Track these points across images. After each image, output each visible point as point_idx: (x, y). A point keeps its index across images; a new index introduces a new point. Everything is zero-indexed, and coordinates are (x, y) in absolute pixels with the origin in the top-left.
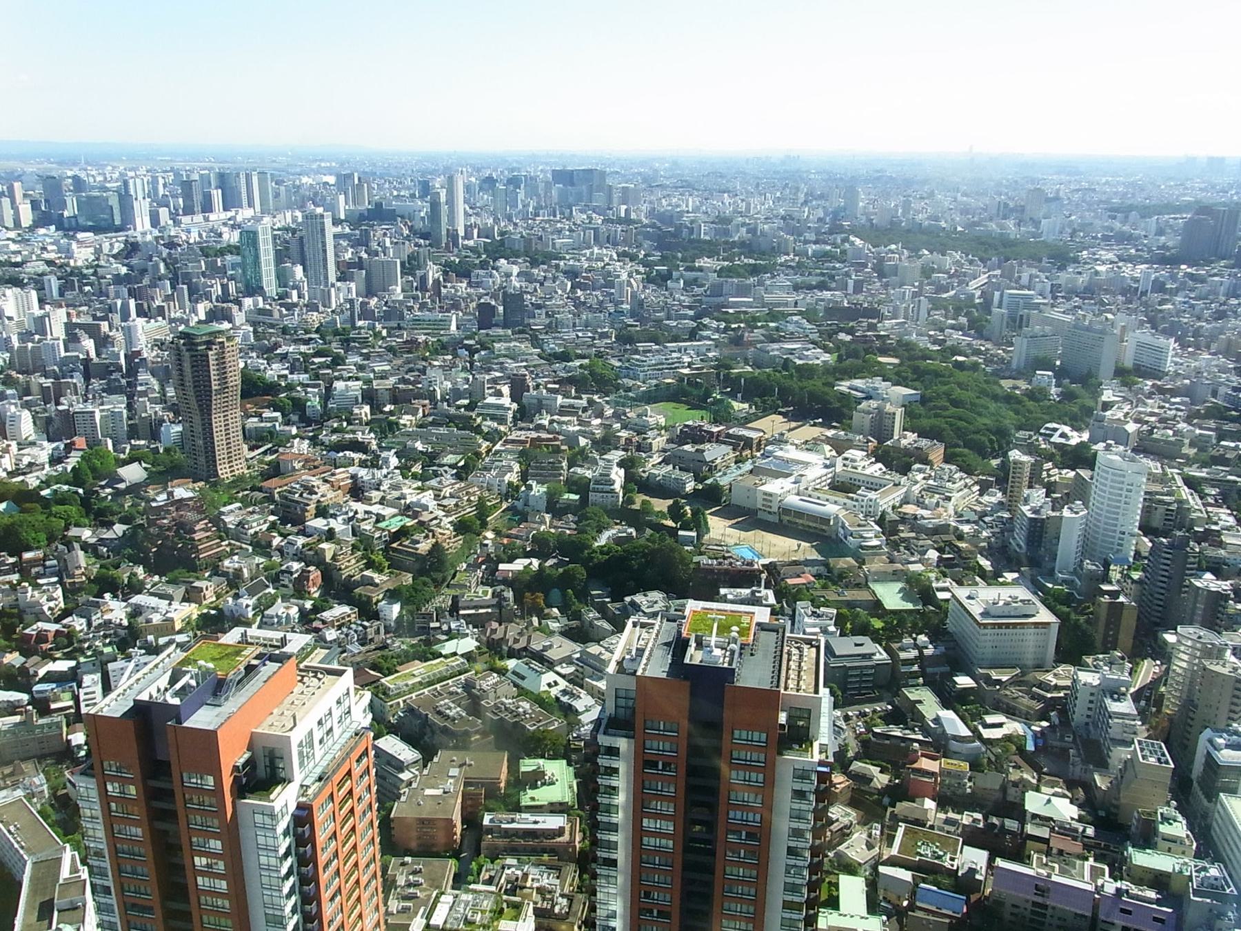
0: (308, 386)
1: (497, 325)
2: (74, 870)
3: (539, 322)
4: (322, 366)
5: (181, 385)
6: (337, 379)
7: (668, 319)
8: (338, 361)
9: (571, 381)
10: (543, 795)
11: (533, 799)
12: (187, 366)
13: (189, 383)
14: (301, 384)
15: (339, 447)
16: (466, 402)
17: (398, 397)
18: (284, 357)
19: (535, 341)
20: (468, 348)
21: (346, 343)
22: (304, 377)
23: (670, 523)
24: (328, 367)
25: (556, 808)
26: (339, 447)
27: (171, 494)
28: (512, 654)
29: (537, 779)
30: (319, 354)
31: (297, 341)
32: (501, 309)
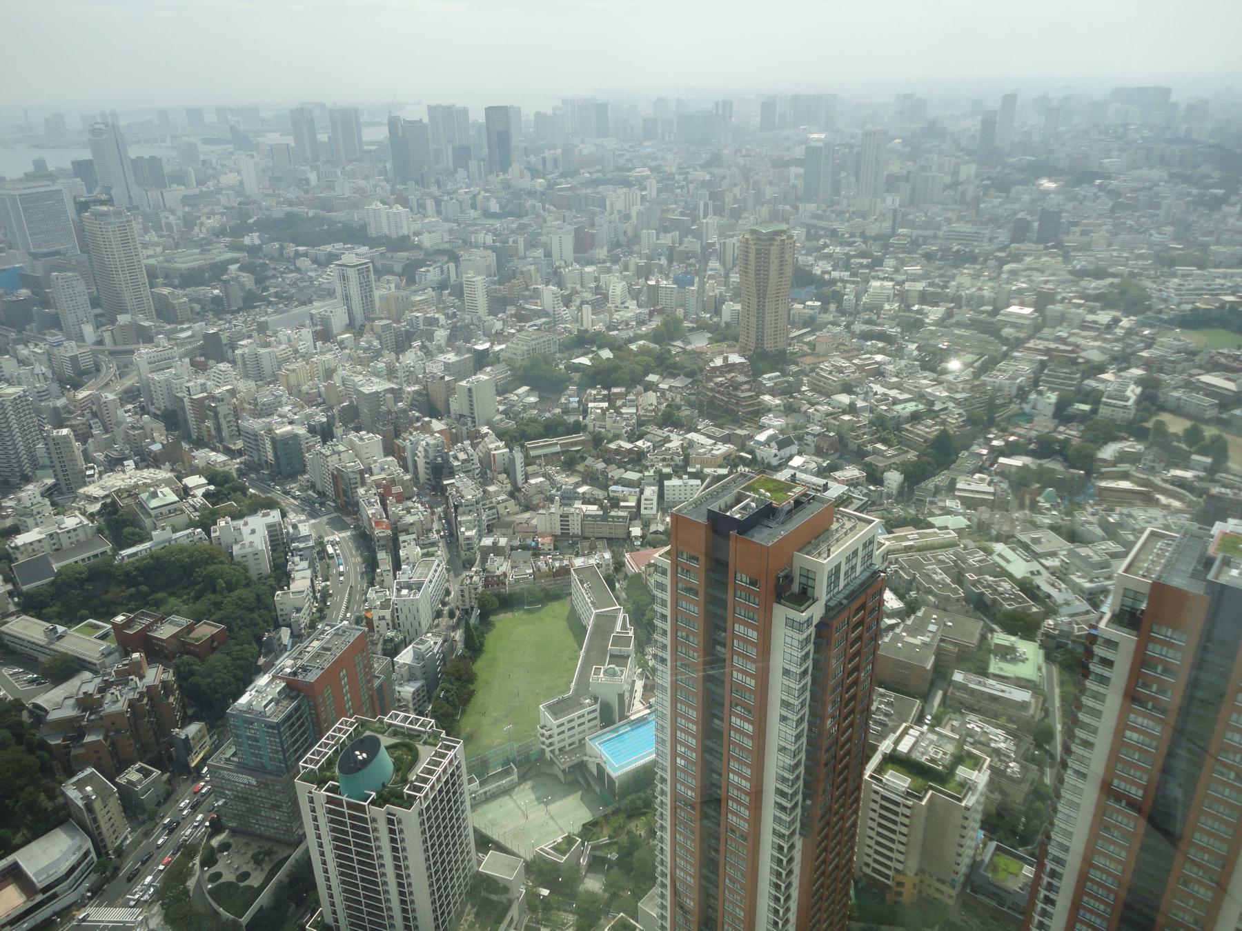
0: (847, 282)
1: (1030, 241)
2: (624, 627)
3: (1070, 241)
4: (862, 266)
5: (745, 272)
6: (874, 278)
7: (1217, 243)
8: (878, 262)
9: (1097, 298)
10: (1010, 670)
11: (1001, 669)
12: (752, 257)
13: (752, 273)
14: (842, 280)
15: (866, 336)
16: (990, 308)
17: (924, 298)
18: (829, 257)
19: (1067, 258)
20: (997, 258)
21: (886, 247)
22: (846, 275)
23: (1184, 446)
24: (866, 267)
25: (1021, 683)
26: (866, 336)
27: (726, 359)
28: (998, 539)
29: (1007, 653)
30: (862, 255)
31: (842, 244)
32: (1036, 224)
